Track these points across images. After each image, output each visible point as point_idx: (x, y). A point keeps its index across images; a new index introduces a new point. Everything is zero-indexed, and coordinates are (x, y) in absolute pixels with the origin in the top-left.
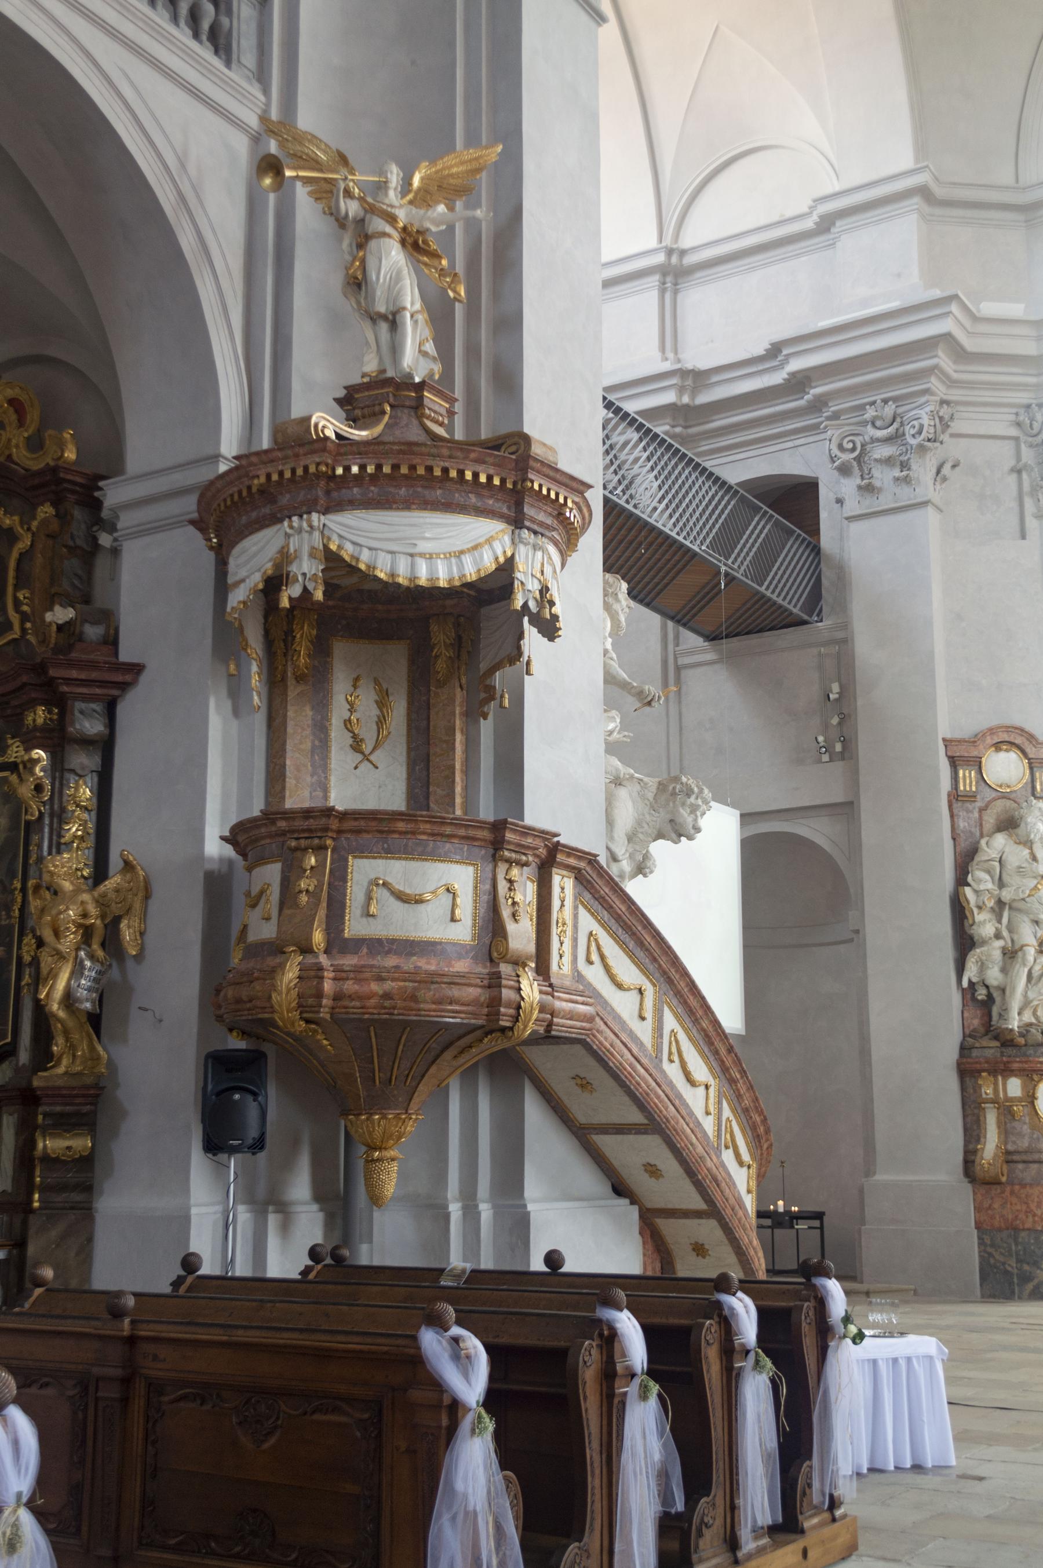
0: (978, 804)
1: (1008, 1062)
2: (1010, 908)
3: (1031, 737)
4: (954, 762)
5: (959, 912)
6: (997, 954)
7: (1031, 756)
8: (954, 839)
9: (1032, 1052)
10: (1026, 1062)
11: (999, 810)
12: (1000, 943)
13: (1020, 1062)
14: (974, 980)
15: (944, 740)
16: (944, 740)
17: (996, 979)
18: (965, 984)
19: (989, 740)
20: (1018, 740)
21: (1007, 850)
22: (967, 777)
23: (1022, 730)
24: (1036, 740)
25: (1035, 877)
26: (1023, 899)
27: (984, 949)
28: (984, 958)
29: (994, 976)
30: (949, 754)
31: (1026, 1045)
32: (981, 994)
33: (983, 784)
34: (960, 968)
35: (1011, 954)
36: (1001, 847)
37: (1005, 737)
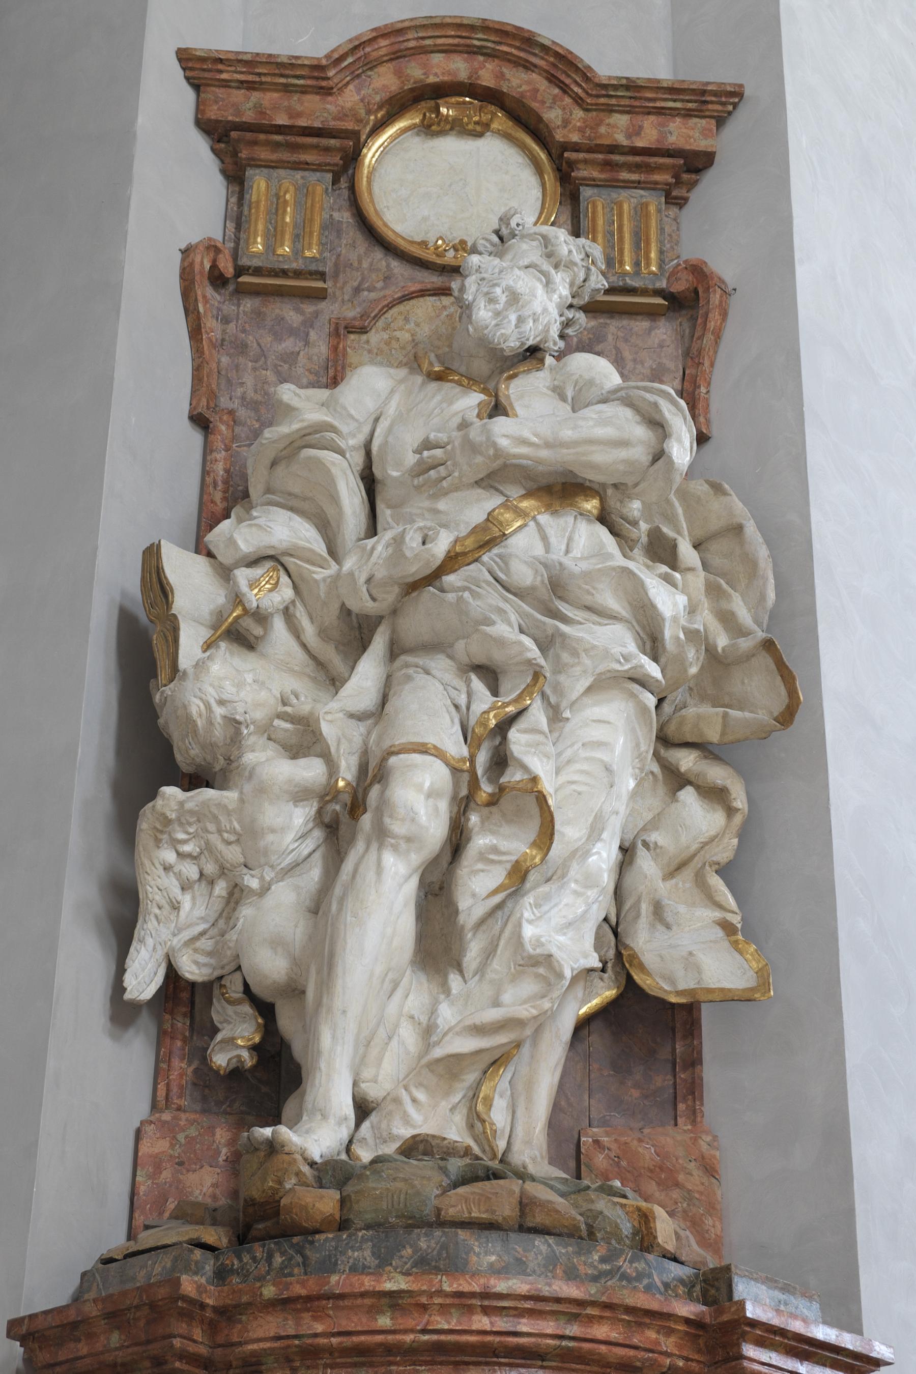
0: (330, 310)
1: (227, 1314)
2: (395, 651)
3: (563, 67)
4: (235, 144)
5: (143, 650)
6: (290, 826)
7: (559, 136)
8: (200, 421)
9: (366, 1255)
10: (310, 1303)
11: (425, 331)
12: (311, 771)
13: (283, 1304)
14: (192, 969)
15: (185, 58)
16: (185, 58)
17: (276, 943)
18: (143, 980)
19: (385, 81)
20: (517, 82)
21: (392, 409)
22: (291, 216)
23: (527, 40)
24: (585, 74)
25: (490, 481)
26: (433, 577)
27: (230, 797)
28: (233, 854)
29: (272, 928)
30: (213, 113)
31: (343, 1225)
32: (235, 1040)
33: (362, 244)
34: (123, 915)
35: (346, 816)
36: (371, 405)
37: (459, 68)
